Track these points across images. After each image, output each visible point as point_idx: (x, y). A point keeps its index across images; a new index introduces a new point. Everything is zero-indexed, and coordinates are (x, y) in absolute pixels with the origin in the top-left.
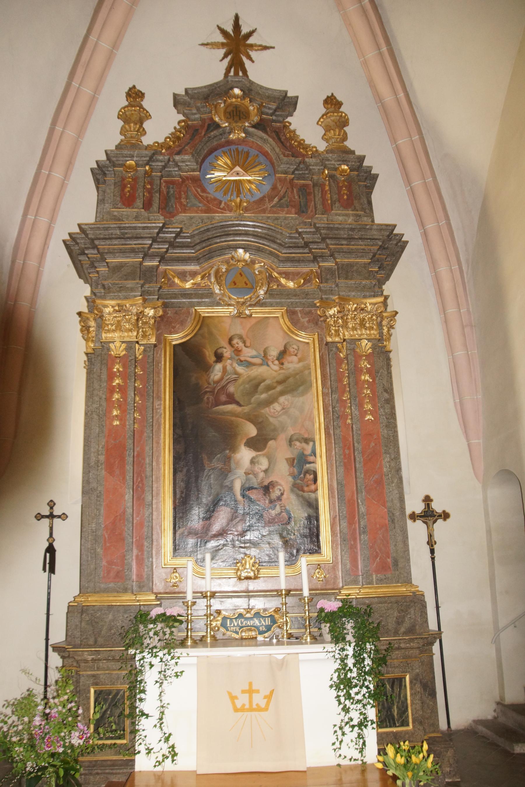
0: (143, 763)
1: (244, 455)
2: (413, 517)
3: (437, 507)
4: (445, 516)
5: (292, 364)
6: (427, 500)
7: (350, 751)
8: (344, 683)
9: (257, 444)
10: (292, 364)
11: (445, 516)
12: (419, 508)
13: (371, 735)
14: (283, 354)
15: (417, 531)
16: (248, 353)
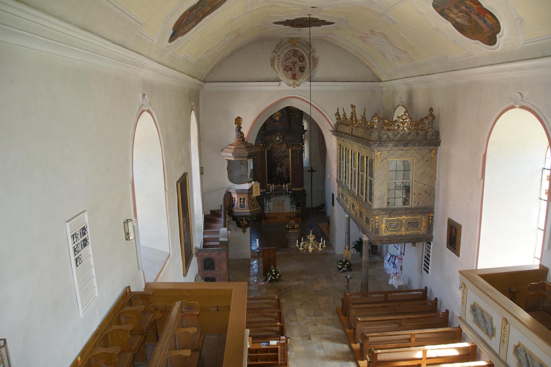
0: (266, 212)
1: (279, 168)
2: (309, 171)
3: (313, 169)
4: (315, 171)
5: (286, 153)
6: (312, 168)
7: (292, 211)
8: (291, 203)
9: (280, 167)
10: (286, 153)
11: (315, 171)
12: (310, 169)
13: (295, 209)
14: (285, 151)
15: (307, 177)
16: (279, 151)
